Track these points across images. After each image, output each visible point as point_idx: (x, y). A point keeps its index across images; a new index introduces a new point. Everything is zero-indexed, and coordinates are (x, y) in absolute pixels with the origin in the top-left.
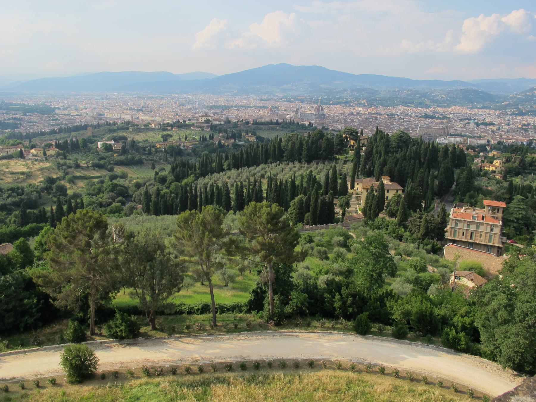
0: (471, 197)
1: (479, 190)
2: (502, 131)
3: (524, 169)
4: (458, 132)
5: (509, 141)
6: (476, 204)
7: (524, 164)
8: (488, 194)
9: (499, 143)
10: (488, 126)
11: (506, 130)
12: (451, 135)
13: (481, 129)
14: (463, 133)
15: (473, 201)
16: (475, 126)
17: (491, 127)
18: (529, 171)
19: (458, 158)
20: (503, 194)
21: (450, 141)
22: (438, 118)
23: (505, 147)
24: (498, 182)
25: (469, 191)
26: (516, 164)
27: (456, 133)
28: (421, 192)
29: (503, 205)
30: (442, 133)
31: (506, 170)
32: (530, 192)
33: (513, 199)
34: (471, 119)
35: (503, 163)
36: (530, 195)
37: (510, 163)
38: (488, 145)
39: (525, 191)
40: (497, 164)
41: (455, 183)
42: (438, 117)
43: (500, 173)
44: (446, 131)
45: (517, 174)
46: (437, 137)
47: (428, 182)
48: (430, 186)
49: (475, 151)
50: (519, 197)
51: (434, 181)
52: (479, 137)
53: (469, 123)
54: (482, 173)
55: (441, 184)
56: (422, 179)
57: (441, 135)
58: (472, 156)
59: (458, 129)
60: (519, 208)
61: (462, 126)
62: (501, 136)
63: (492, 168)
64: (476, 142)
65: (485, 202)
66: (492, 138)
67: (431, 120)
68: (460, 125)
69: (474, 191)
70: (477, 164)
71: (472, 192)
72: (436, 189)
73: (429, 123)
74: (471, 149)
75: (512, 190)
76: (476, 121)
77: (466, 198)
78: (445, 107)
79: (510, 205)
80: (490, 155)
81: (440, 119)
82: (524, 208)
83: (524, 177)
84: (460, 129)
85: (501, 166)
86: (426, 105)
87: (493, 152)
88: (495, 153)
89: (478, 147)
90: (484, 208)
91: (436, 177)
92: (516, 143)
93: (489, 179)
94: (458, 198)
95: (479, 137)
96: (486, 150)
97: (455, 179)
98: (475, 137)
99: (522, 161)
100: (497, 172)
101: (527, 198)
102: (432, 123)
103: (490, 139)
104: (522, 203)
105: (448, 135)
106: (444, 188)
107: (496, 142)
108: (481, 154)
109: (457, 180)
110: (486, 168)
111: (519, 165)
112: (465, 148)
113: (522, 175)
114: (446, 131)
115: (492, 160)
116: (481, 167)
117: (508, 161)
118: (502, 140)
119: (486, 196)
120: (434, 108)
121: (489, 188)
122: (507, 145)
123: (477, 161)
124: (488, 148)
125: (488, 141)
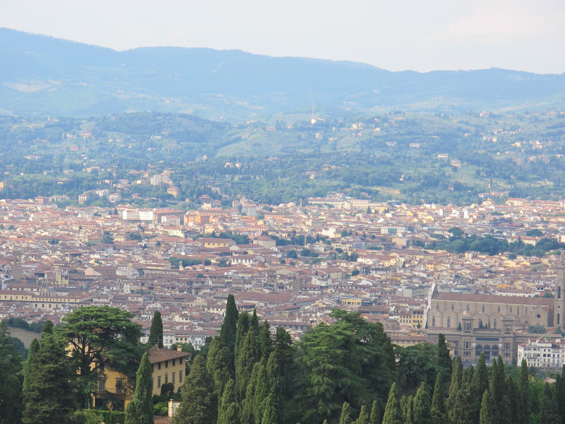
22: (516, 249)
30: (543, 321)
42: (520, 244)
46: (517, 340)
57: (537, 330)
67: (485, 260)
73: (478, 273)
78: (546, 195)
81: (528, 251)
86: (458, 187)
102: (493, 274)
120: (497, 201)
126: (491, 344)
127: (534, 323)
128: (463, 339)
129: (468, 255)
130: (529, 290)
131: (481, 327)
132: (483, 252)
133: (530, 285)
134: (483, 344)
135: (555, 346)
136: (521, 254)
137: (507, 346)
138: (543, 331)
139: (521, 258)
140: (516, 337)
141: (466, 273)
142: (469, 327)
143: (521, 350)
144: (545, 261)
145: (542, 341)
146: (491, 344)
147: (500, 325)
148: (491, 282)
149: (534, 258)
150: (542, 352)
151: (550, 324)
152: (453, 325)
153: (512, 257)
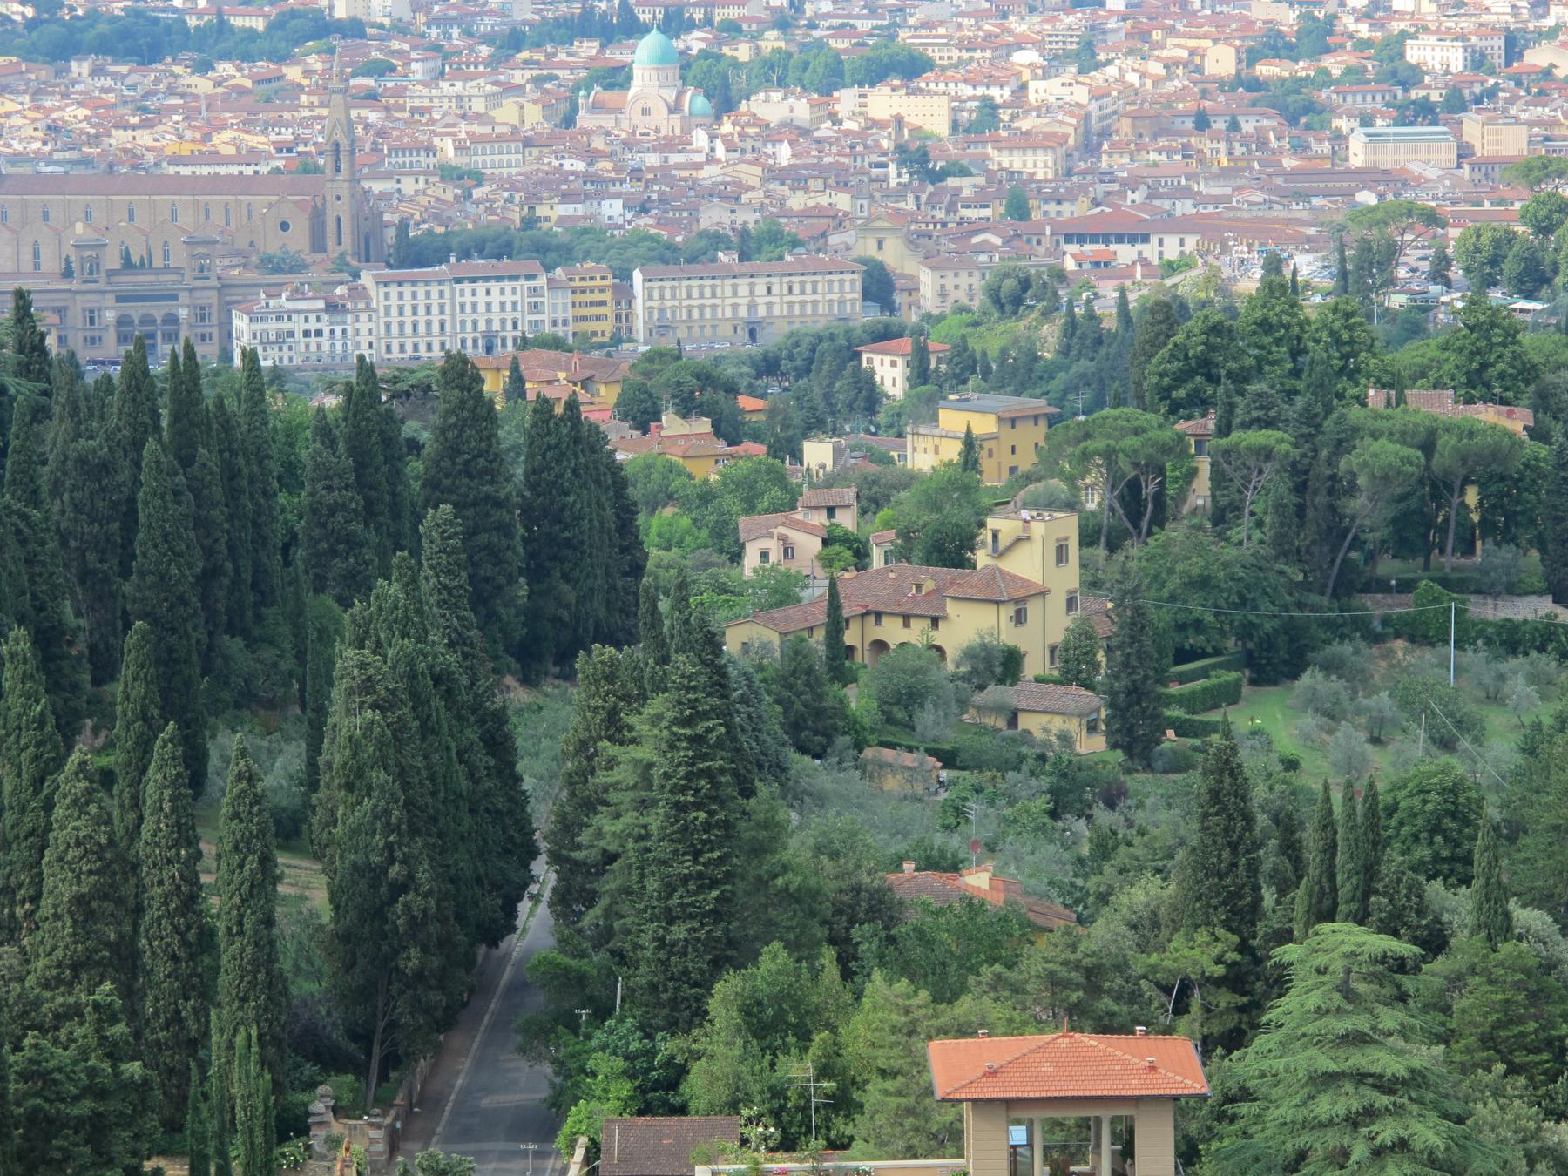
0: (772, 1026)
1: (853, 926)
2: (1028, 142)
3: (1349, 584)
4: (489, 207)
5: (1125, 253)
6: (843, 1103)
7: (1337, 531)
8: (959, 962)
9: (1012, 297)
10: (846, 100)
11: (1068, 126)
12: (414, 255)
13: (770, 134)
14: (554, 212)
15: (798, 1069)
16: (694, 101)
17: (884, 102)
18: (1401, 606)
19: (520, 528)
20: (1148, 928)
21: (403, 325)
23: (1083, 335)
24: (1070, 791)
25: (731, 954)
26: (1247, 541)
27: (470, 219)
28: (115, 1054)
29: (1168, 1063)
30: (298, 240)
31: (1136, 624)
32: (1456, 869)
33: (1280, 983)
34: (632, 28)
35: (1088, 538)
36: (1457, 906)
37: (1174, 533)
38: (883, 336)
39: (1394, 860)
40: (1028, 565)
41: (544, 873)
43: (1073, 666)
44: (339, 209)
45: (1274, 661)
46: (230, 296)
47: (189, 898)
48: (231, 954)
49: (729, 429)
50: (1349, 939)
51: (267, 876)
52: (759, 246)
53: (617, 77)
54: (858, 700)
55: (367, 902)
56: (113, 887)
58: (707, 496)
59: (481, 160)
60: (1360, 1077)
61: (534, 116)
62: (1019, 209)
63: (966, 627)
64: (721, 311)
65: (952, 1065)
66: (917, 241)
67: (126, 78)
68: (507, 113)
69: (801, 948)
70: (782, 593)
71: (773, 960)
72: (312, 988)
74: (687, 408)
75: (1248, 870)
76: (695, 42)
77: (717, 1054)
79: (1247, 1064)
80: (927, 454)
81: (244, 48)
82: (1417, 1079)
83: (1358, 679)
84: (508, 163)
85: (1070, 577)
87: (953, 420)
88: (984, 425)
89: (768, 366)
90: (949, 1140)
91: (289, 829)
92: (1212, 278)
93: (949, 759)
94: (604, 1064)
95: (759, 246)
96: (868, 396)
97: (542, 817)
98: (717, 240)
99: (1312, 490)
100: (1034, 665)
101: (1435, 942)
103: (894, 255)
104: (1389, 1018)
105: (368, 250)
106: (412, 960)
107: (968, 287)
109: (568, 828)
110: (893, 632)
111: (1283, 548)
112: (608, 395)
113: (1329, 667)
114: (339, 209)
115: (959, 515)
116: (836, 624)
117: (1141, 504)
118: (1038, 260)
119: (946, 994)
121: (978, 880)
122: (1107, 307)
124: (889, 372)
125: (879, 286)
126: (158, 311)
127: (272, 244)
128: (80, 303)
129: (80, 68)
130: (253, 156)
131: (128, 264)
132: (120, 57)
133: (256, 141)
134: (136, 311)
135: (332, 307)
136: (225, 56)
137: (202, 314)
138: (297, 267)
139: (225, 68)
140: (224, 287)
141: (75, 115)
142: (95, 266)
143: (240, 323)
144: (293, 73)
145: (298, 294)
146: (158, 311)
147: (179, 258)
148: (146, 138)
149: (263, 66)
150: (298, 325)
151: (318, 245)
152: (51, 264)
153: (203, 67)
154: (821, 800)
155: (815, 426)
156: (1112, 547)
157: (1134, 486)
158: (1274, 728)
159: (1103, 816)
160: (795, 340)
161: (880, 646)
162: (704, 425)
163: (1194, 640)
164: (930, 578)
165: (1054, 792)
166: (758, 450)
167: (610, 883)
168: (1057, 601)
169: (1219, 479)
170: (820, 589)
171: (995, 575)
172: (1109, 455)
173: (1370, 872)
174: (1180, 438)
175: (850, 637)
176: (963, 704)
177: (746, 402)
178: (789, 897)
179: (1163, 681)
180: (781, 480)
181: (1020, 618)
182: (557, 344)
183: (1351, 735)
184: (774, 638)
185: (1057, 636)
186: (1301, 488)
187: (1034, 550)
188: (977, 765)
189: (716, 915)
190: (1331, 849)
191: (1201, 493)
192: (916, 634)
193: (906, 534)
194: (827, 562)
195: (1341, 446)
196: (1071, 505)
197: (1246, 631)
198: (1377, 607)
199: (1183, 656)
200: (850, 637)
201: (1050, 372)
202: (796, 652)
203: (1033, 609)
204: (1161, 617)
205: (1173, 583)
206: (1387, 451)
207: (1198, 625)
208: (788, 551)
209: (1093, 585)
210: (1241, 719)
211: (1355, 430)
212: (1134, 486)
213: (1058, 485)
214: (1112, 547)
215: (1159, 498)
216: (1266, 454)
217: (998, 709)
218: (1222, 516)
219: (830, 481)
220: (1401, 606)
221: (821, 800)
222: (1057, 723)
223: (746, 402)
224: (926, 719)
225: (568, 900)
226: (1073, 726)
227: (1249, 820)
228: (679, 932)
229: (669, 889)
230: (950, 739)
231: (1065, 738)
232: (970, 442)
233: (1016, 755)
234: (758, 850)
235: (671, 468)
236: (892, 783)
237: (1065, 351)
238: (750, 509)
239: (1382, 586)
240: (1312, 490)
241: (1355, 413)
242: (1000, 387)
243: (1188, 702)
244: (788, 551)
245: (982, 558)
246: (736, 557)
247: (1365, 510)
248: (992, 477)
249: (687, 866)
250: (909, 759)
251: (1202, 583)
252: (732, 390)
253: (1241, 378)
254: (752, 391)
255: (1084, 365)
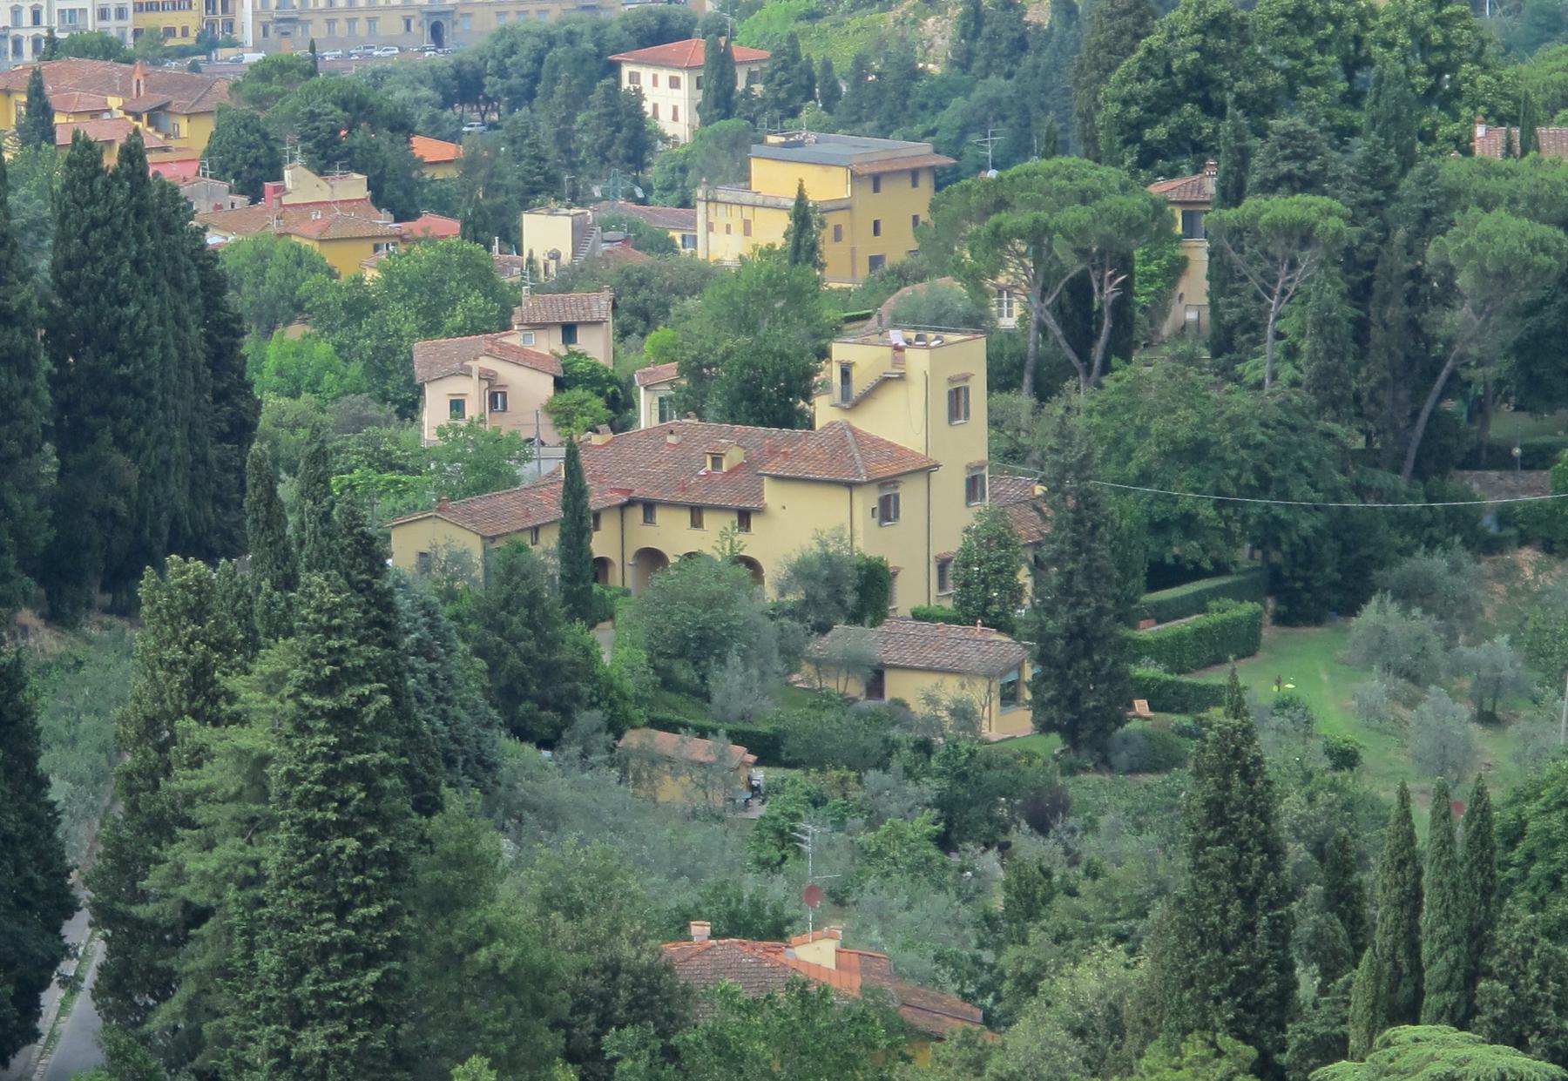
3: (1442, 454)
7: (1421, 365)
18: (1531, 492)
24: (973, 804)
26: (1270, 381)
31: (1083, 522)
35: (1002, 377)
37: (1147, 368)
40: (900, 422)
41: (86, 940)
43: (977, 592)
45: (1315, 584)
49: (397, 194)
54: (614, 649)
58: (358, 307)
63: (798, 526)
70: (486, 469)
74: (326, 158)
80: (730, 235)
83: (1457, 614)
85: (972, 442)
87: (774, 178)
89: (464, 86)
93: (767, 750)
96: (632, 137)
97: (82, 846)
99: (1381, 297)
100: (912, 590)
108: (546, 233)
109: (125, 864)
110: (673, 535)
111: (1331, 393)
112: (194, 135)
113: (1411, 594)
115: (785, 337)
116: (578, 521)
117: (1090, 320)
121: (816, 952)
123: (485, 388)
124: (668, 97)
154: (553, 818)
155: (542, 187)
156: (1043, 392)
157: (1080, 290)
158: (1315, 696)
159: (1028, 846)
160: (508, 43)
161: (652, 558)
162: (355, 186)
163: (1181, 549)
164: (736, 444)
165: (946, 805)
166: (445, 227)
167: (195, 959)
168: (951, 483)
169: (1223, 277)
170: (549, 463)
171: (844, 439)
172: (1038, 236)
173: (1477, 938)
174: (1158, 208)
175: (602, 544)
176: (792, 655)
177: (425, 147)
178: (496, 980)
179: (1130, 619)
180: (484, 279)
181: (887, 511)
182: (107, 49)
183: (1446, 710)
184: (473, 546)
185: (950, 542)
186: (1360, 293)
187: (910, 395)
188: (814, 759)
189: (376, 1012)
190: (1412, 900)
191: (1192, 300)
192: (712, 538)
193: (695, 371)
194: (562, 416)
195: (1429, 222)
196: (974, 321)
197: (1268, 533)
198: (1490, 492)
199: (1162, 575)
200: (602, 544)
201: (939, 97)
202: (511, 568)
203: (910, 496)
204: (1125, 510)
205: (1145, 454)
206: (1505, 230)
207: (1188, 525)
208: (497, 398)
209: (1010, 455)
210: (1261, 681)
211: (1453, 195)
212: (1080, 290)
213: (953, 288)
214: (1043, 392)
215: (1121, 310)
216: (1303, 235)
217: (850, 665)
218: (1229, 339)
219: (568, 281)
220: (1531, 492)
221: (553, 818)
222: (950, 689)
223: (425, 147)
224: (730, 681)
225: (128, 985)
226: (978, 693)
227: (1274, 851)
228: (313, 1041)
229: (296, 969)
230: (770, 716)
231: (964, 715)
232: (803, 215)
233: (877, 744)
234: (447, 903)
235: (300, 259)
236: (672, 790)
237: (963, 61)
238: (432, 328)
239: (1498, 458)
240: (1381, 297)
241: (1452, 166)
242: (853, 122)
243: (1172, 653)
244: (497, 398)
245: (823, 410)
246: (410, 409)
247: (1468, 328)
248: (840, 273)
249: (327, 930)
250: (700, 749)
251: (1196, 452)
252: (402, 126)
253: (1260, 107)
254: (436, 130)
255: (996, 85)
